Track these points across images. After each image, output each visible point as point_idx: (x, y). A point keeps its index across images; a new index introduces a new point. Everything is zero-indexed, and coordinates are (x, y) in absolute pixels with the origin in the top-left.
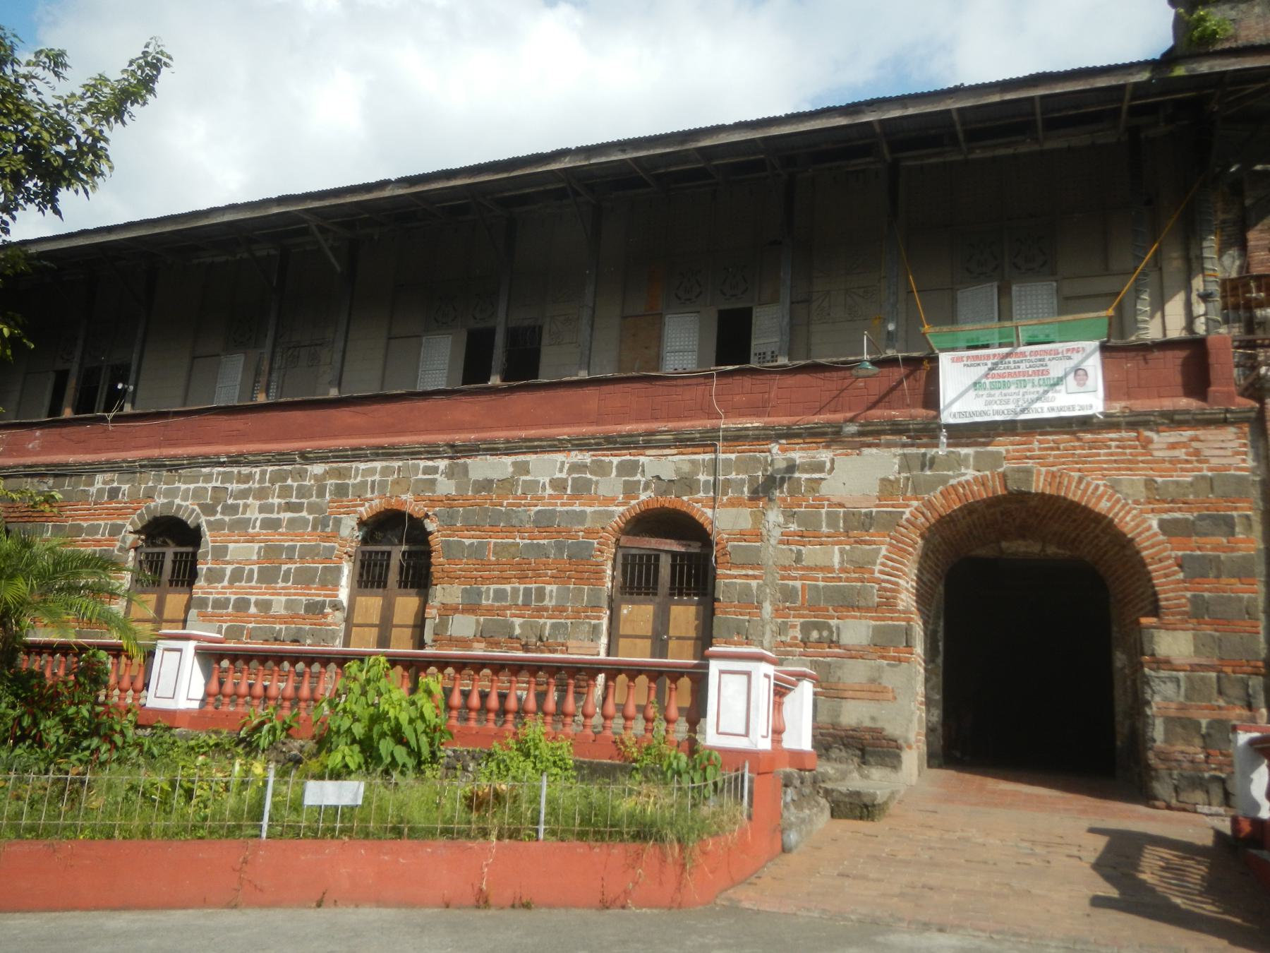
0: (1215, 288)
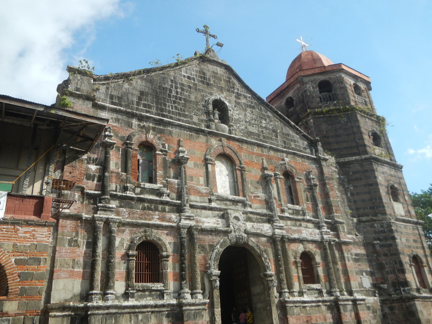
0: (50, 181)
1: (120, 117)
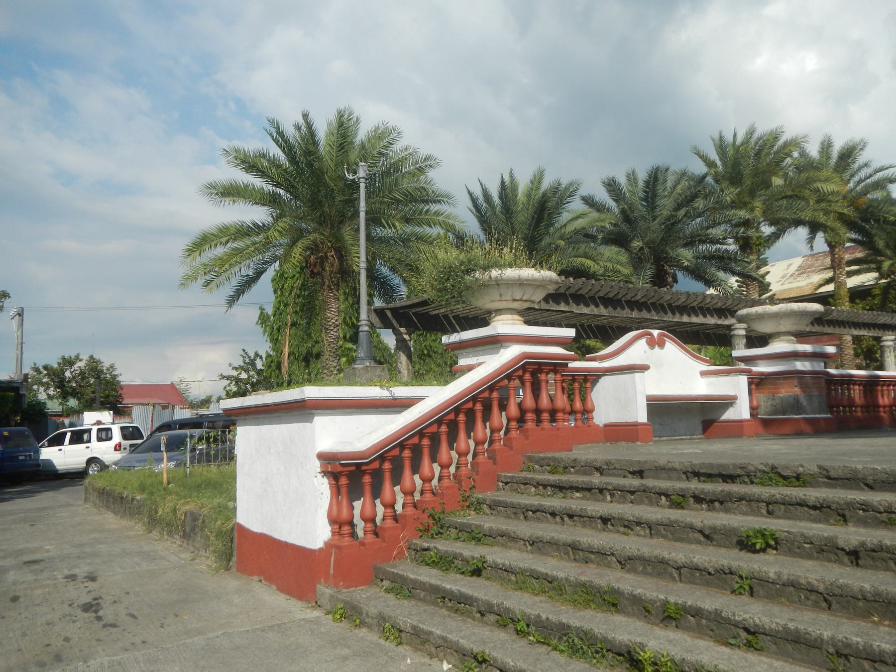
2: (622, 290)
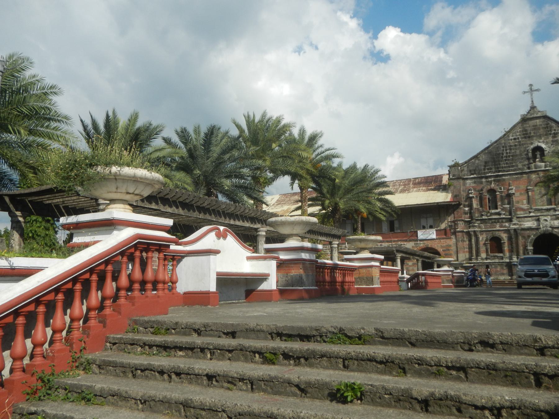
1: (476, 180)
2: (195, 199)
